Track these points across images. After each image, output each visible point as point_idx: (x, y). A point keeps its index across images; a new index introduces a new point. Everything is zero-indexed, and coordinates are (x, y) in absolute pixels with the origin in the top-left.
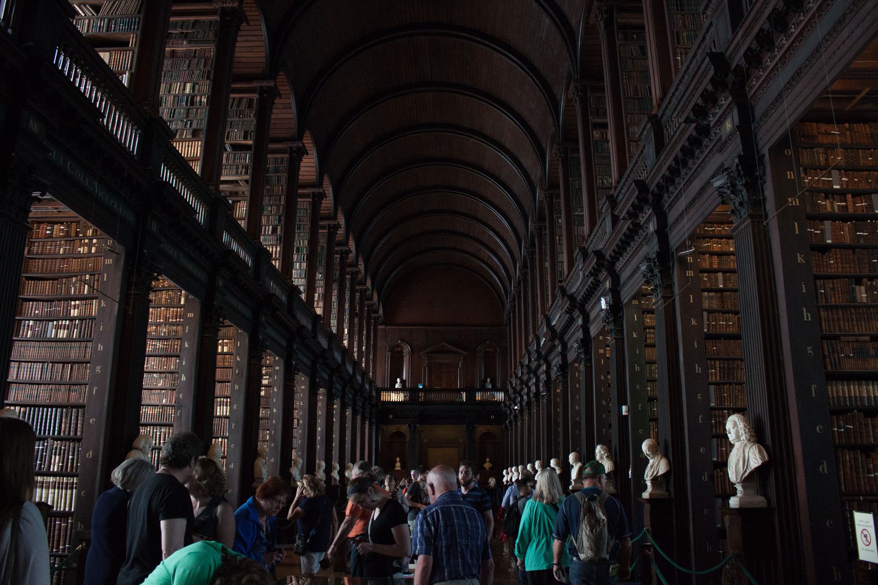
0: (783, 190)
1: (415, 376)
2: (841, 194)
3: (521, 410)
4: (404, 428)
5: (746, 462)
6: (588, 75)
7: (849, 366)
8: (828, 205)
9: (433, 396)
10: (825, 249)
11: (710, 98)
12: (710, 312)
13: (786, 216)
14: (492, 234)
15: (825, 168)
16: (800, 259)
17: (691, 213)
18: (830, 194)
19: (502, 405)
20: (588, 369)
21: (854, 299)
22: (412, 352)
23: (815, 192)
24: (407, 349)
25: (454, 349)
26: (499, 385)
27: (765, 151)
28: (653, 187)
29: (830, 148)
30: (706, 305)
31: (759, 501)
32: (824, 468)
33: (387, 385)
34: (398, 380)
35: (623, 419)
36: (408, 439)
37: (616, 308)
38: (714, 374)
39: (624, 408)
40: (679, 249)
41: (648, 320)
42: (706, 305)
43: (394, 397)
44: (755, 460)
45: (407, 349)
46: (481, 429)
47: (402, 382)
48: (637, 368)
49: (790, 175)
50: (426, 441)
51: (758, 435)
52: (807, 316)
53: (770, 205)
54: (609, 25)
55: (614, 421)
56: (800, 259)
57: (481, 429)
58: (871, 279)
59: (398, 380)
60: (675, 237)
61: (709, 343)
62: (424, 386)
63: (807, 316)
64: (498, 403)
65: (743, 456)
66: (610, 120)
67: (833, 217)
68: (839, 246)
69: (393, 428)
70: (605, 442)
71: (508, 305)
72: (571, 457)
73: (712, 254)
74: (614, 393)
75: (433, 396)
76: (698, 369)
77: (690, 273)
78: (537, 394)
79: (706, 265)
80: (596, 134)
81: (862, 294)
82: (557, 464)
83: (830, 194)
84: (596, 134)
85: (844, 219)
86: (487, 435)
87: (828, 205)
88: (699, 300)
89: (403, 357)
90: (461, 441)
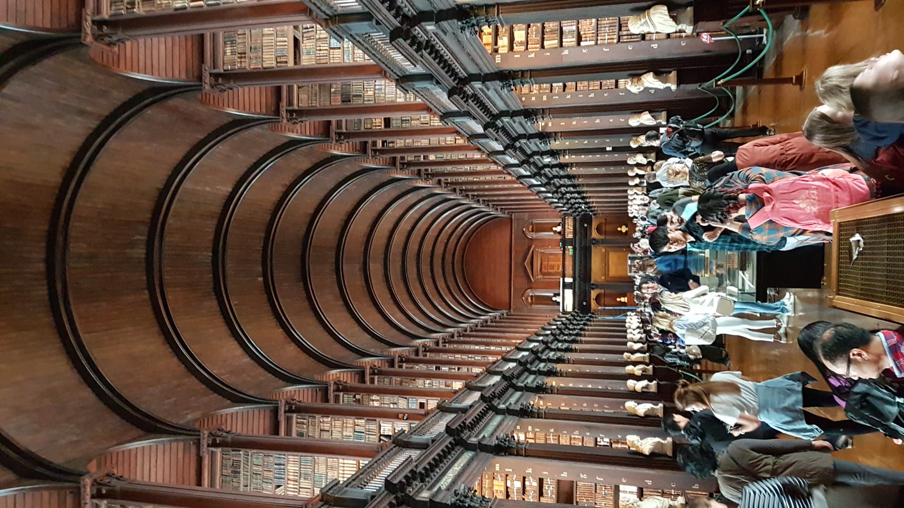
3: (586, 203)
4: (594, 294)
5: (648, 120)
16: (569, 97)
26: (559, 221)
39: (608, 149)
45: (530, 293)
46: (595, 234)
47: (555, 295)
49: (533, 99)
50: (603, 278)
56: (569, 97)
57: (595, 234)
59: (554, 299)
69: (593, 304)
71: (499, 214)
77: (550, 124)
78: (579, 193)
86: (599, 230)
89: (536, 296)
90: (603, 250)
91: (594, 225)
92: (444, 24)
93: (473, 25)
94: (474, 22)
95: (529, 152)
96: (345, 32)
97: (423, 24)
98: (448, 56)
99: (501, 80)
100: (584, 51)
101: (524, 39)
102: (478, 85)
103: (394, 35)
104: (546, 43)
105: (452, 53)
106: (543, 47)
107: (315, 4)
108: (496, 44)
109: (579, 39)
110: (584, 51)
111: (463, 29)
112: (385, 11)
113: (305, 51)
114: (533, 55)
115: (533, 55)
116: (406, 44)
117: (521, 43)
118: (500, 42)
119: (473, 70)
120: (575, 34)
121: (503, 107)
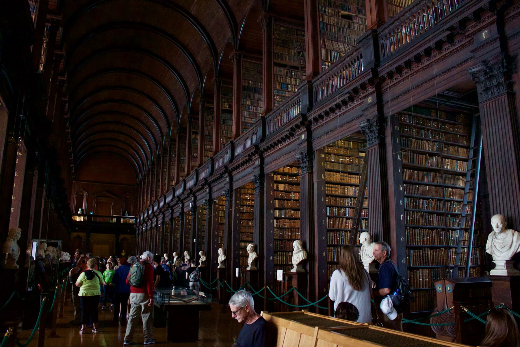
0: (237, 199)
1: (89, 207)
2: (249, 200)
3: (146, 230)
4: (82, 235)
5: (221, 259)
6: (193, 114)
7: (245, 239)
8: (246, 203)
9: (98, 219)
10: (243, 213)
11: (223, 173)
12: (221, 217)
13: (237, 205)
14: (137, 144)
15: (247, 194)
17: (218, 192)
18: (247, 200)
19: (135, 226)
20: (182, 223)
21: (248, 224)
22: (88, 196)
23: (243, 199)
24: (85, 194)
25: (110, 195)
27: (234, 189)
28: (209, 181)
29: (248, 189)
30: (220, 215)
31: (224, 267)
32: (237, 260)
33: (74, 212)
34: (80, 209)
35: (194, 243)
36: (83, 240)
37: (195, 207)
38: (220, 234)
39: (194, 240)
40: (214, 199)
41: (205, 212)
42: (220, 215)
43: (79, 219)
44: (223, 259)
45: (85, 194)
47: (82, 210)
48: (200, 227)
51: (225, 253)
52: (237, 228)
53: (233, 202)
54: (203, 106)
55: (191, 243)
58: (252, 220)
59: (80, 209)
60: (214, 195)
61: (220, 226)
62: (93, 213)
63: (237, 228)
64: (132, 225)
65: (221, 257)
66: (199, 131)
67: (246, 206)
68: (247, 212)
69: (75, 234)
70: (188, 250)
72: (174, 254)
73: (224, 200)
74: (191, 232)
75: (98, 219)
76: (216, 233)
79: (221, 203)
80: (193, 136)
81: (250, 224)
82: (167, 256)
83: (247, 200)
84: (193, 136)
85: (249, 206)
86: (125, 239)
87: (246, 203)
88: (218, 213)
91: (127, 236)
92: (305, 144)
93: (303, 159)
94: (305, 160)
95: (197, 194)
96: (302, 91)
97: (306, 133)
98: (280, 146)
99: (260, 175)
100: (271, 221)
101: (280, 189)
102: (257, 163)
103: (304, 116)
104: (277, 201)
105: (281, 148)
106: (275, 199)
107: (321, 77)
108: (279, 174)
109: (277, 219)
110: (271, 221)
111: (302, 154)
112: (319, 113)
113: (281, 69)
114: (271, 193)
115: (271, 193)
116: (298, 122)
117: (278, 188)
118: (279, 176)
119: (266, 160)
120: (280, 217)
121: (235, 178)
